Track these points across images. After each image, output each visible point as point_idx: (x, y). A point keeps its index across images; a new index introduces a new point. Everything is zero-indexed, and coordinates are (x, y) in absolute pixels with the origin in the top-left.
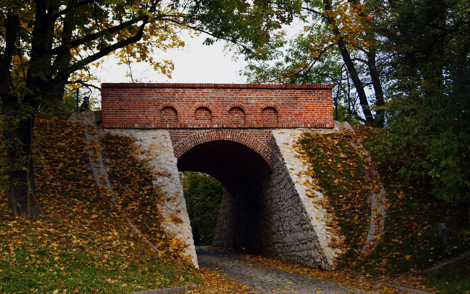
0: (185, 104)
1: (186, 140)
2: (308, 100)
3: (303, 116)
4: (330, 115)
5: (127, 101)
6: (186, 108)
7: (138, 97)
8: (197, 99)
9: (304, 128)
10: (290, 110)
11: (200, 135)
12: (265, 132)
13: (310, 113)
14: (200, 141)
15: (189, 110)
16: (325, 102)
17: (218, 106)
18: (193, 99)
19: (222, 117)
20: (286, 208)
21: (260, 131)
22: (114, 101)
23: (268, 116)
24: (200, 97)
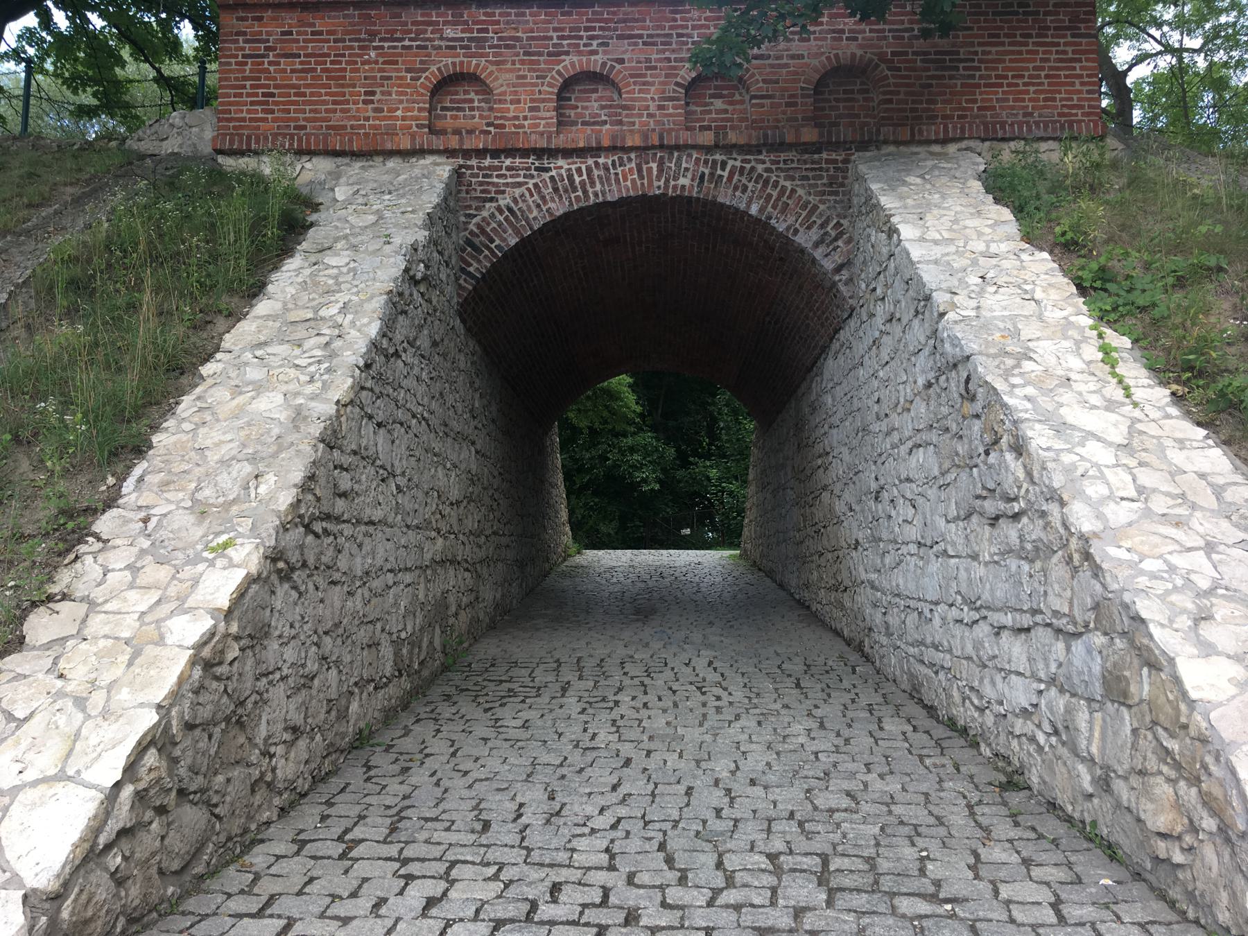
0: (522, 62)
1: (522, 195)
2: (998, 36)
3: (979, 97)
4: (1089, 92)
5: (306, 56)
6: (524, 77)
7: (350, 40)
8: (569, 45)
9: (983, 140)
10: (929, 77)
11: (576, 177)
12: (828, 161)
13: (1009, 85)
14: (577, 198)
15: (536, 85)
16: (1066, 44)
17: (648, 68)
18: (554, 45)
19: (660, 107)
20: (901, 442)
21: (806, 156)
22: (263, 56)
23: (841, 105)
24: (581, 38)
